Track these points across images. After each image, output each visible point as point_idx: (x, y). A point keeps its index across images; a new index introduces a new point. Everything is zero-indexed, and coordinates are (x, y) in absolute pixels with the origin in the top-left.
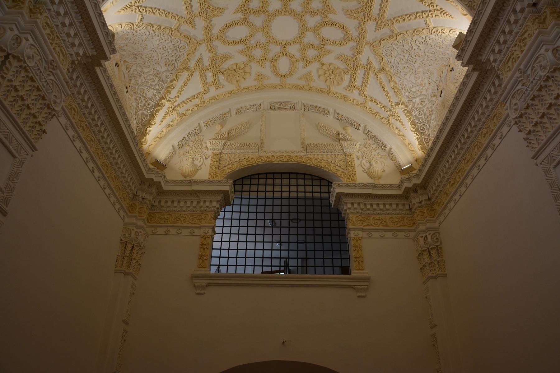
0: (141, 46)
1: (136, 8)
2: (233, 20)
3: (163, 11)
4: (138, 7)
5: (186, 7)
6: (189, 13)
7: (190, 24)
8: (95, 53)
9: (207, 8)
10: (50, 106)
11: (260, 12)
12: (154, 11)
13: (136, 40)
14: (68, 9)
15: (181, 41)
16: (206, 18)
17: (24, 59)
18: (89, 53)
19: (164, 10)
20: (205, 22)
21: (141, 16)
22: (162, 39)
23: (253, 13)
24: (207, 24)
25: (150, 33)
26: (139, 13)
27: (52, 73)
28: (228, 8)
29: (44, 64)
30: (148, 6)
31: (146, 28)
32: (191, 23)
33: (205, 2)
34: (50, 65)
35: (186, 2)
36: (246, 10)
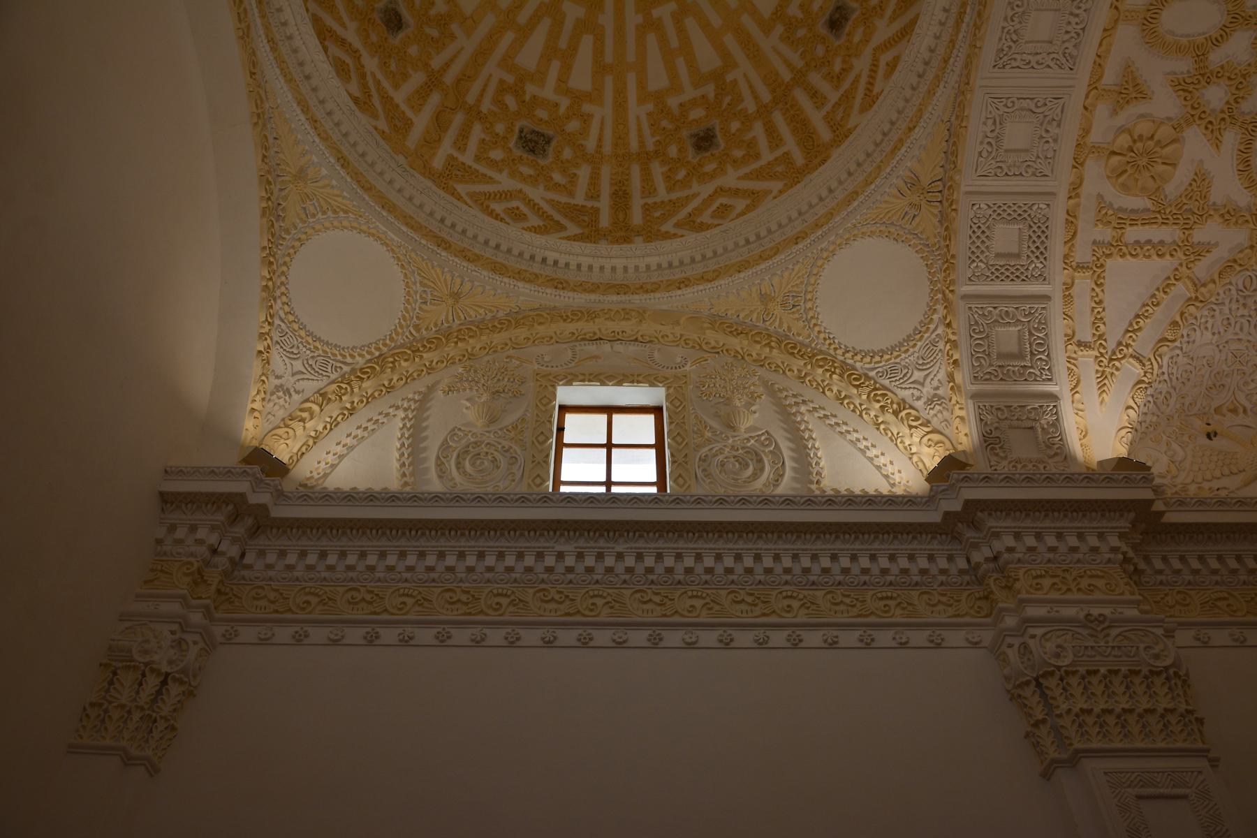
0: (1199, 370)
1: (1110, 365)
3: (1144, 309)
4: (1111, 360)
5: (1158, 255)
6: (1174, 253)
7: (1199, 255)
8: (1132, 515)
9: (1180, 208)
10: (1154, 669)
11: (1240, 86)
12: (1136, 327)
13: (1179, 376)
14: (1033, 528)
15: (1231, 283)
16: (1201, 216)
17: (1055, 666)
18: (1125, 528)
19: (1144, 305)
20: (1209, 221)
21: (1131, 360)
22: (1207, 322)
23: (1238, 103)
24: (1216, 217)
25: (1179, 345)
26: (1122, 362)
27: (1109, 627)
28: (1201, 161)
29: (1085, 632)
30: (1119, 337)
31: (1160, 356)
32: (1197, 252)
33: (1165, 213)
34: (1092, 625)
35: (1147, 254)
36: (1223, 119)
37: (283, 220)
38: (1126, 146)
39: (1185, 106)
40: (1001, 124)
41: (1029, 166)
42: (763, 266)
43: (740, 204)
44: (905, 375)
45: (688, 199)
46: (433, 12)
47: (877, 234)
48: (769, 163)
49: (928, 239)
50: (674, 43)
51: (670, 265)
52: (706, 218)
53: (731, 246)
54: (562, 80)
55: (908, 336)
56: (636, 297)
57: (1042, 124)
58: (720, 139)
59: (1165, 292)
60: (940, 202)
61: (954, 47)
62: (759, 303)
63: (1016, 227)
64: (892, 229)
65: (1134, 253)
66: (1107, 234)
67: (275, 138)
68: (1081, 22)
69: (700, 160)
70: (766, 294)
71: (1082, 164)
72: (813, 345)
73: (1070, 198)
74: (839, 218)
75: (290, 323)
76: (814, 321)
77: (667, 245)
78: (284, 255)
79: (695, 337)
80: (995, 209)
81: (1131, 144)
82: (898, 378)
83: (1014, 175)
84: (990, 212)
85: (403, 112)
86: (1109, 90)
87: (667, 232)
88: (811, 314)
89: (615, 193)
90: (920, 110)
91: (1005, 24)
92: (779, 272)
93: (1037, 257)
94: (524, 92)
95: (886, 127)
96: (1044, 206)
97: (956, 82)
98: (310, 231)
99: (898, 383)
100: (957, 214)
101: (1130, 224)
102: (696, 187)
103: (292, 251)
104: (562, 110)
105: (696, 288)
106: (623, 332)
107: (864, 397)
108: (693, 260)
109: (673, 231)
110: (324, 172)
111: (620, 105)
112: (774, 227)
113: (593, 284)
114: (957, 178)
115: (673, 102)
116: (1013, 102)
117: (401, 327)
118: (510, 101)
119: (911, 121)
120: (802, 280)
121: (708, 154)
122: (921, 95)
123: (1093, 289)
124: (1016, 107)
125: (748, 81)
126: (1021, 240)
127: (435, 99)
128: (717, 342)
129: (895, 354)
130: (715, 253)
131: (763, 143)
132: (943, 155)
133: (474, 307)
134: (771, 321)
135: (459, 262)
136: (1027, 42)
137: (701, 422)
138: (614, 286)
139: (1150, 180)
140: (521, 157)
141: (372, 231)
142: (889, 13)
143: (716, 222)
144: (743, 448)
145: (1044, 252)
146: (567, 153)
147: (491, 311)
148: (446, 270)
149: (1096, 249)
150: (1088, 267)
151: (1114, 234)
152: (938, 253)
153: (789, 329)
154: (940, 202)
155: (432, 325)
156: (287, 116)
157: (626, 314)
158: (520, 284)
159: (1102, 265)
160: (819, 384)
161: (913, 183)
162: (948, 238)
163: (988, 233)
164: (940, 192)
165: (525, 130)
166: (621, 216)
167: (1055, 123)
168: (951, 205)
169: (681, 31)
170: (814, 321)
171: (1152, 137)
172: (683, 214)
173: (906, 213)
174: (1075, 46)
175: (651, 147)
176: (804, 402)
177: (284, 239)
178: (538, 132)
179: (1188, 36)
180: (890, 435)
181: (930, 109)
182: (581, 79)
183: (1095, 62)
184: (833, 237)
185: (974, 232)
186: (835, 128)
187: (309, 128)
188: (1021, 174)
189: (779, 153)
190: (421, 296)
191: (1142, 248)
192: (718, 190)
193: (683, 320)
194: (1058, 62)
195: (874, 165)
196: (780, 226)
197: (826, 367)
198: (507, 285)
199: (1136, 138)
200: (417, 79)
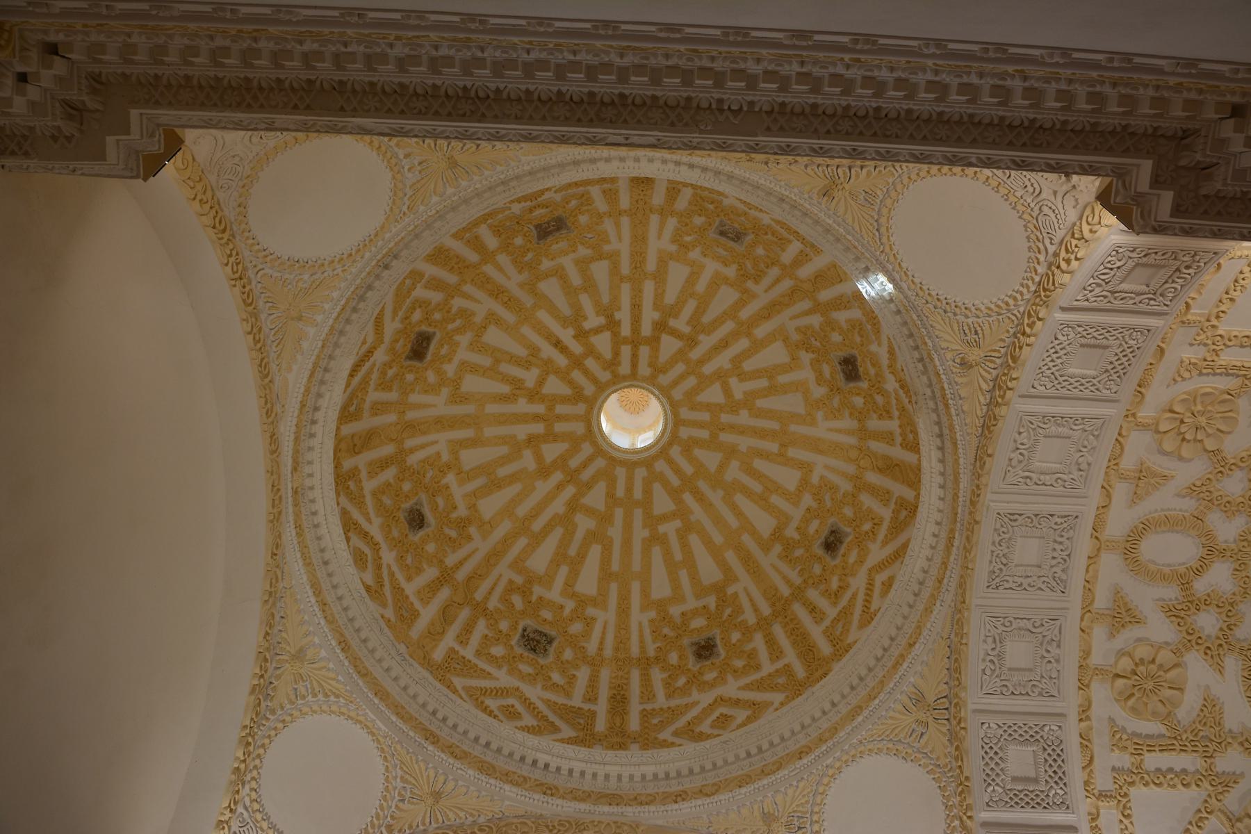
2: (1241, 679)
5: (1183, 785)
6: (1200, 783)
7: (1226, 786)
9: (1196, 735)
11: (1230, 614)
16: (1220, 743)
20: (1229, 749)
23: (1231, 629)
24: (1236, 745)
28: (1208, 687)
32: (1225, 782)
33: (1181, 740)
35: (1171, 783)
36: (1220, 645)
37: (271, 700)
38: (1129, 669)
39: (1180, 631)
40: (1001, 642)
41: (1034, 685)
42: (765, 782)
43: (741, 715)
45: (688, 707)
46: (454, 515)
47: (885, 751)
48: (770, 675)
49: (938, 759)
50: (678, 556)
51: (667, 775)
52: (705, 727)
53: (731, 759)
54: (569, 584)
56: (629, 809)
57: (1041, 644)
58: (721, 649)
59: (1199, 827)
60: (948, 719)
61: (946, 568)
62: (761, 823)
63: (1029, 749)
64: (900, 747)
65: (1158, 782)
66: (1124, 760)
67: (282, 617)
68: (1066, 549)
69: (700, 668)
70: (769, 812)
71: (1088, 686)
73: (1081, 720)
74: (844, 733)
75: (253, 812)
77: (665, 754)
78: (264, 736)
80: (1006, 728)
81: (1134, 667)
83: (1021, 694)
84: (1001, 732)
85: (412, 604)
86: (1103, 614)
87: (665, 741)
89: (613, 697)
90: (919, 627)
91: (994, 549)
92: (782, 789)
93: (1056, 782)
94: (531, 593)
95: (886, 643)
96: (1055, 728)
97: (953, 600)
98: (296, 713)
100: (966, 733)
101: (1148, 751)
102: (695, 695)
103: (273, 733)
104: (567, 611)
105: (694, 802)
108: (691, 771)
109: (671, 739)
110: (323, 653)
111: (624, 611)
112: (776, 740)
113: (584, 792)
114: (963, 695)
115: (675, 611)
116: (1010, 622)
117: (373, 826)
118: (517, 601)
119: (911, 637)
120: (806, 799)
121: (708, 663)
122: (919, 613)
123: (1121, 821)
124: (1014, 627)
125: (748, 595)
126: (1036, 764)
127: (444, 594)
130: (714, 765)
132: (946, 672)
135: (445, 758)
136: (1016, 566)
138: (607, 796)
139: (1159, 704)
140: (521, 655)
141: (360, 718)
142: (881, 537)
143: (716, 732)
145: (1063, 777)
146: (568, 654)
147: (472, 815)
148: (431, 765)
149: (1117, 776)
150: (1111, 796)
151: (1133, 760)
152: (951, 774)
154: (948, 719)
155: (406, 827)
156: (299, 597)
158: (507, 787)
159: (1126, 795)
161: (918, 699)
162: (959, 758)
163: (1001, 754)
164: (947, 709)
165: (529, 630)
167: (1055, 644)
168: (959, 722)
169: (685, 546)
171: (1153, 661)
172: (681, 722)
173: (913, 730)
174: (1063, 571)
175: (651, 652)
177: (268, 719)
178: (541, 632)
179: (1169, 565)
182: (587, 583)
183: (1084, 587)
184: (838, 754)
185: (986, 752)
186: (835, 642)
187: (317, 610)
188: (1027, 693)
189: (779, 665)
190: (399, 793)
191: (1165, 777)
192: (719, 699)
194: (1049, 585)
195: (877, 680)
196: (783, 739)
198: (493, 787)
199: (1138, 661)
200: (431, 573)
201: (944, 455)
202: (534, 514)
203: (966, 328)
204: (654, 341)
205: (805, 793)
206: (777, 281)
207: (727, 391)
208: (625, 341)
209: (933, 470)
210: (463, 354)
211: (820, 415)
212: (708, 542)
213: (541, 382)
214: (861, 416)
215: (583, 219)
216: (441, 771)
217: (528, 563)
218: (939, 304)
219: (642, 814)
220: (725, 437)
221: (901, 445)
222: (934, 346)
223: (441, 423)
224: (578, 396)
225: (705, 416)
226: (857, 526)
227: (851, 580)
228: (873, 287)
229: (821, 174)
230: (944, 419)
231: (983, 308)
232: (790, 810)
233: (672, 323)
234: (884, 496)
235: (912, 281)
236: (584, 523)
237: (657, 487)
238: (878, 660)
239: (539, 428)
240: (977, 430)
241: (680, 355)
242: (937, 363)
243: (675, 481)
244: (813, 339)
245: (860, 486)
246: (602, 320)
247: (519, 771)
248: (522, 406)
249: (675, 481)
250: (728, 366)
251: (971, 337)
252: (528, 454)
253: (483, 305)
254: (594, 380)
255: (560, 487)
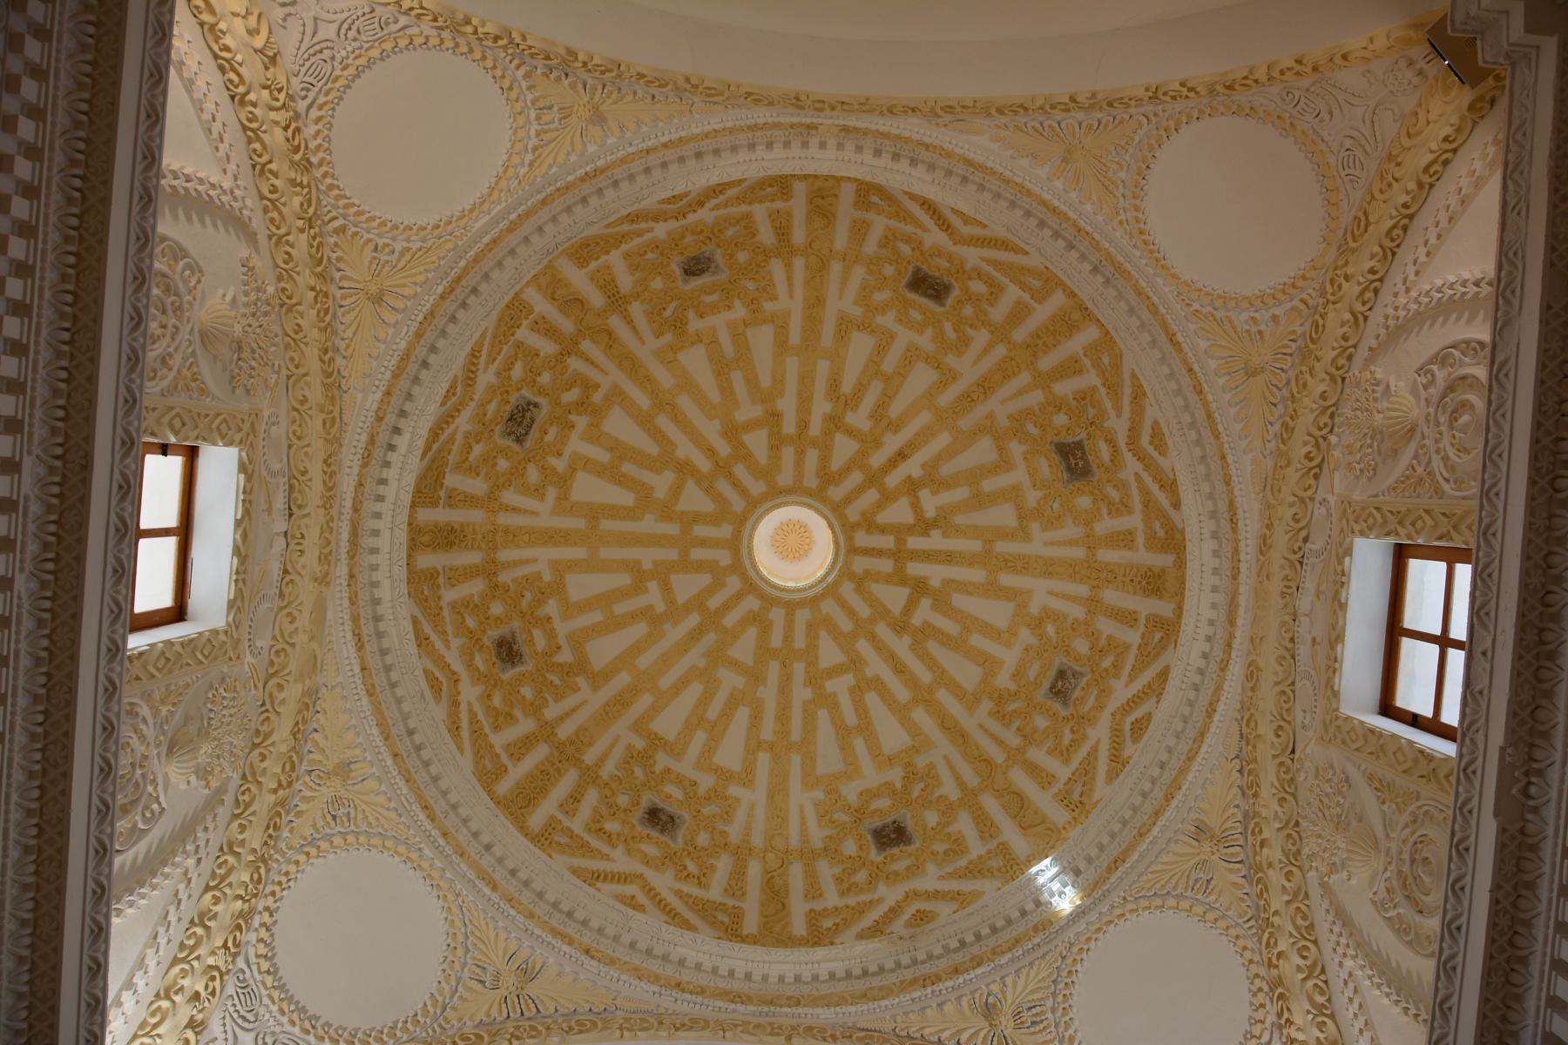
37: (545, 74)
44: (243, 1018)
46: (691, 314)
47: (451, 931)
49: (453, 1008)
50: (620, 609)
54: (587, 464)
55: (304, 1007)
58: (509, 674)
61: (698, 993)
62: (336, 761)
64: (460, 952)
67: (653, 97)
70: (351, 771)
72: (276, 856)
75: (395, 38)
76: (313, 851)
78: (495, 60)
79: (292, 667)
82: (239, 1007)
85: (597, 259)
88: (324, 845)
92: (383, 788)
94: (579, 414)
95: (580, 915)
97: (667, 1009)
98: (518, 107)
99: (232, 1009)
102: (456, 643)
103: (498, 73)
106: (302, 552)
107: (211, 961)
110: (592, 148)
111: (552, 537)
115: (552, 607)
117: (346, 206)
119: (598, 951)
120: (374, 823)
121: (494, 659)
125: (579, 706)
127: (597, 299)
128: (283, 702)
129: (276, 994)
131: (513, 733)
133: (356, 323)
134: (311, 784)
137: (180, 694)
141: (496, 193)
144: (143, 775)
146: (503, 464)
147: (348, 346)
148: (419, 290)
152: (438, 1030)
153: (300, 814)
155: (340, 253)
156: (675, 121)
157: (325, 558)
158: (379, 395)
160: (223, 878)
161: (527, 973)
164: (522, 1014)
165: (535, 411)
166: (426, 539)
169: (633, 617)
170: (313, 851)
172: (428, 629)
175: (505, 577)
176: (199, 860)
177: (518, 67)
178: (530, 427)
180: (153, 1021)
181: (624, 977)
182: (587, 488)
184: (439, 864)
187: (650, 143)
190: (388, 245)
192: (456, 677)
193: (314, 645)
197: (251, 886)
198: (380, 376)
200: (626, 282)
201: (840, 980)
202: (677, 417)
203: (1038, 1009)
204: (900, 578)
205: (382, 821)
206: (1000, 743)
207: (834, 672)
208: (900, 541)
209: (816, 966)
210: (904, 337)
211: (819, 794)
212: (637, 649)
213: (851, 432)
214: (830, 850)
215: (1084, 502)
216: (409, 304)
217: (616, 410)
218: (1064, 974)
219: (338, 588)
220: (774, 668)
221: (812, 910)
222: (1001, 966)
223: (815, 304)
224: (828, 478)
225: (800, 642)
226: (689, 853)
227: (621, 848)
228: (1052, 880)
229: (1228, 824)
230: (890, 979)
231: (1071, 1032)
232: (357, 802)
233: (925, 603)
234: (736, 886)
235: (1090, 938)
236: (661, 483)
237: (705, 579)
238: (555, 905)
239: (789, 427)
240: (902, 1030)
241: (881, 612)
242: (979, 971)
243: (713, 603)
244: (922, 785)
245: (741, 854)
246: (930, 513)
247: (390, 409)
248: (821, 407)
249: (713, 603)
250: (869, 673)
251: (1027, 1016)
252: (757, 411)
253: (968, 368)
254: (848, 501)
255: (711, 452)
